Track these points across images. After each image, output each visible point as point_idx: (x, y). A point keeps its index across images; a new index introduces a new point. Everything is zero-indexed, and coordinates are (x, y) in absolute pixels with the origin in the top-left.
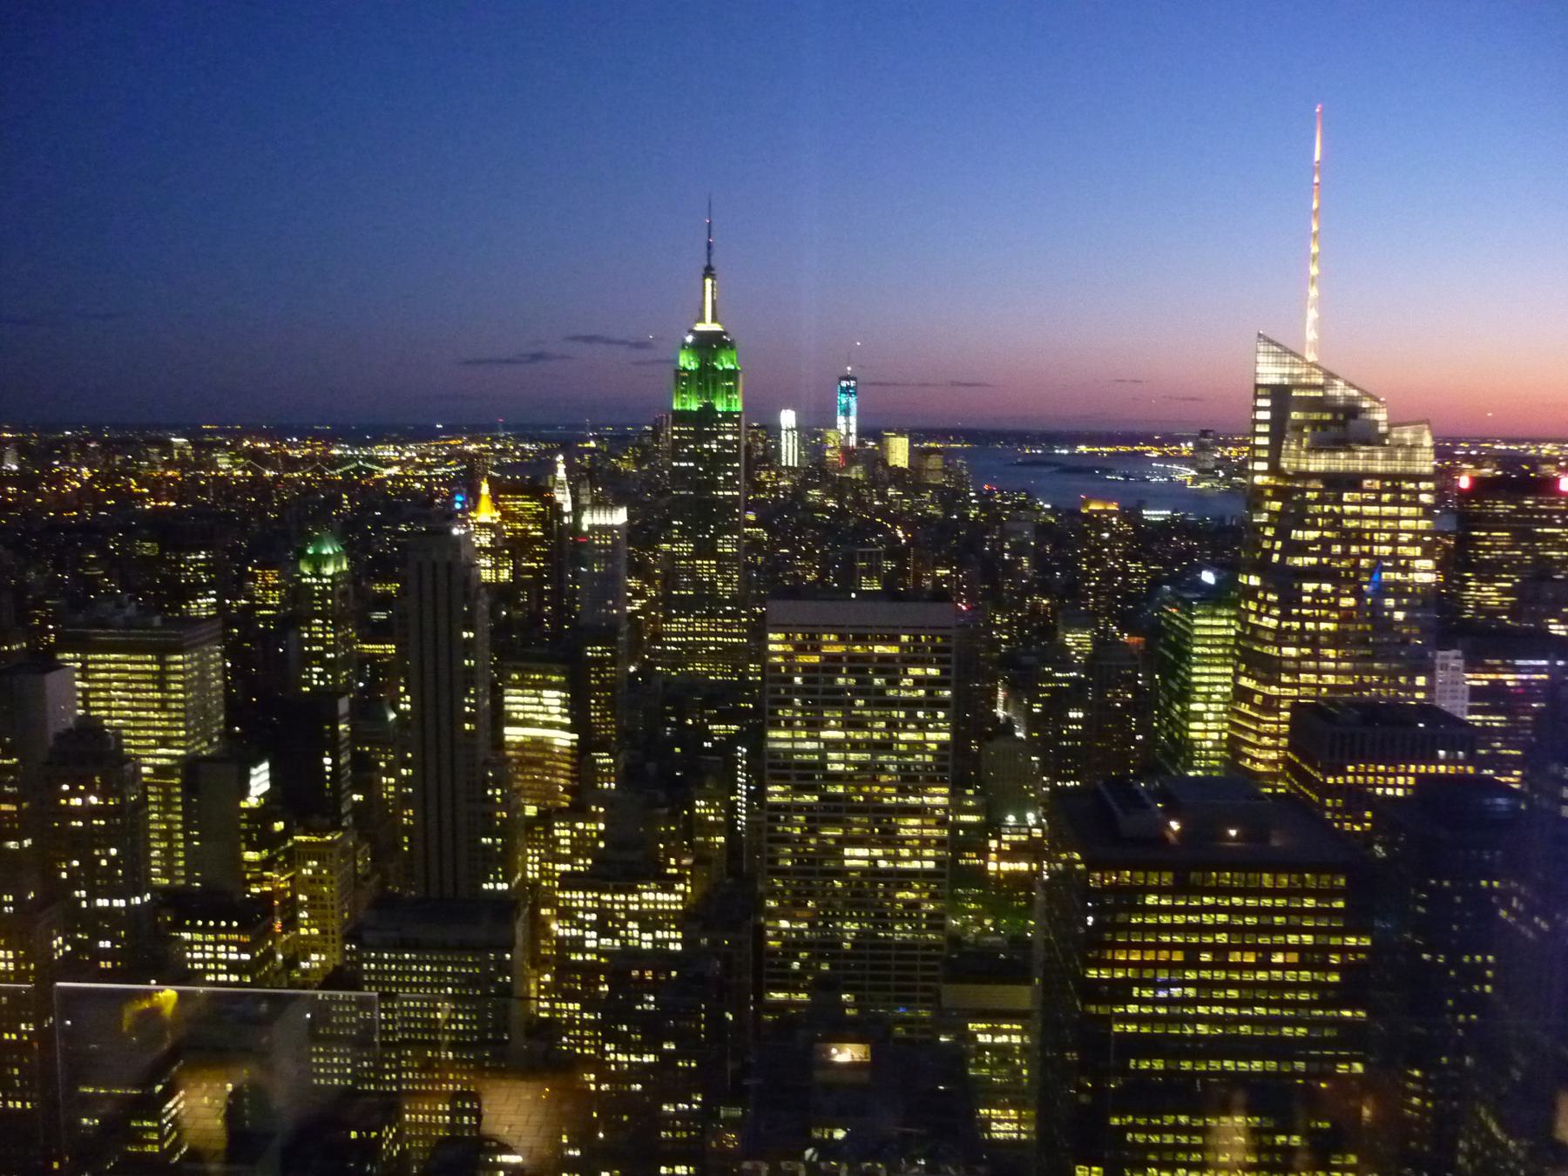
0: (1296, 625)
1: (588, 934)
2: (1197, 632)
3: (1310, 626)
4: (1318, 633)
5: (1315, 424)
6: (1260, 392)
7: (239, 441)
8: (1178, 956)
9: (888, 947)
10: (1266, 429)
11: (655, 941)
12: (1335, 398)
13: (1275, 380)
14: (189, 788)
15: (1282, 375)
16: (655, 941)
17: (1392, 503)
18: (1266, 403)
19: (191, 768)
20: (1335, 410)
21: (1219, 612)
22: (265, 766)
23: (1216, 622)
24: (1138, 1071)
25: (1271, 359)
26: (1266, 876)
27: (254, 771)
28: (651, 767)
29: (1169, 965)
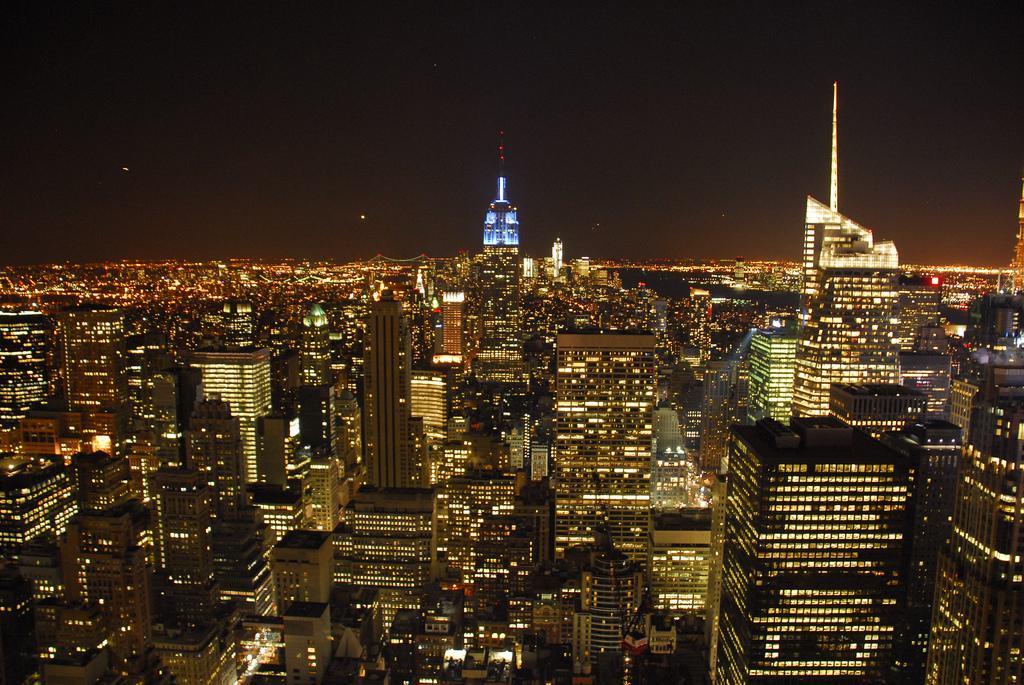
0: (829, 346)
1: (465, 507)
2: (773, 351)
3: (836, 346)
4: (841, 350)
5: (836, 243)
6: (809, 227)
8: (808, 508)
9: (620, 513)
10: (812, 245)
14: (260, 432)
16: (500, 511)
17: (877, 283)
18: (812, 232)
20: (847, 236)
21: (784, 341)
22: (297, 421)
25: (815, 210)
26: (854, 466)
27: (291, 423)
29: (804, 513)
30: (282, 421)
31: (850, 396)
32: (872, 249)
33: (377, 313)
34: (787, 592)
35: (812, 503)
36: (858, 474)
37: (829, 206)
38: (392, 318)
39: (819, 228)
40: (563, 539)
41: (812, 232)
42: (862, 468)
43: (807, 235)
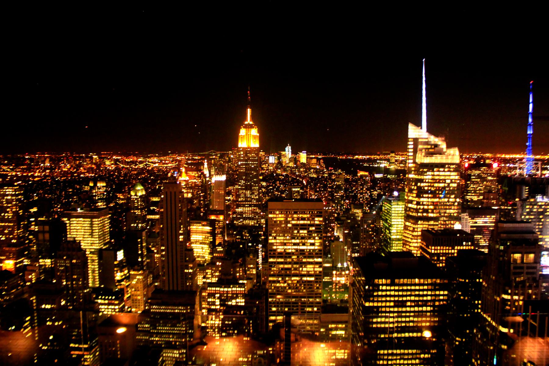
0: (422, 207)
3: (426, 207)
5: (426, 149)
7: (112, 157)
11: (236, 302)
12: (430, 142)
13: (414, 137)
14: (100, 258)
15: (416, 135)
17: (449, 171)
19: (100, 253)
20: (431, 145)
22: (122, 251)
23: (398, 206)
24: (380, 338)
27: (118, 253)
28: (233, 251)
29: (390, 307)
30: (113, 252)
31: (430, 236)
32: (446, 152)
33: (167, 190)
34: (382, 352)
35: (394, 301)
36: (419, 285)
37: (421, 128)
38: (175, 193)
39: (416, 140)
40: (273, 318)
41: (412, 143)
42: (422, 281)
43: (409, 145)
